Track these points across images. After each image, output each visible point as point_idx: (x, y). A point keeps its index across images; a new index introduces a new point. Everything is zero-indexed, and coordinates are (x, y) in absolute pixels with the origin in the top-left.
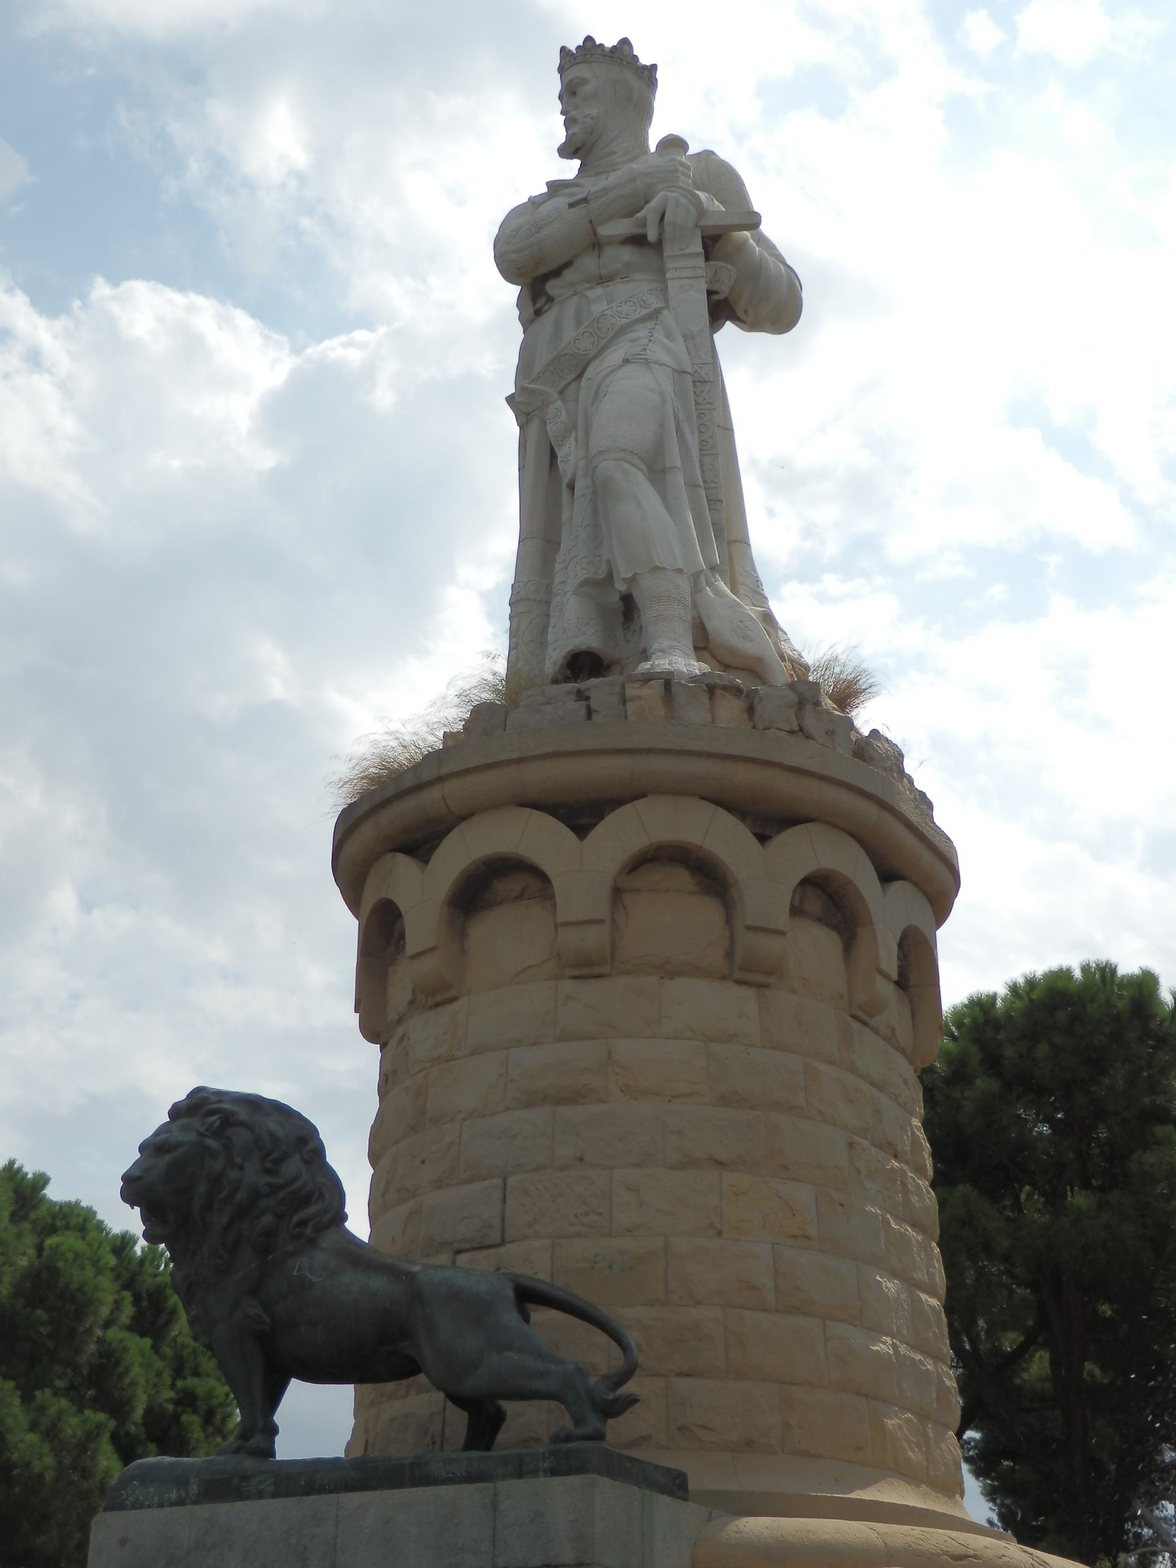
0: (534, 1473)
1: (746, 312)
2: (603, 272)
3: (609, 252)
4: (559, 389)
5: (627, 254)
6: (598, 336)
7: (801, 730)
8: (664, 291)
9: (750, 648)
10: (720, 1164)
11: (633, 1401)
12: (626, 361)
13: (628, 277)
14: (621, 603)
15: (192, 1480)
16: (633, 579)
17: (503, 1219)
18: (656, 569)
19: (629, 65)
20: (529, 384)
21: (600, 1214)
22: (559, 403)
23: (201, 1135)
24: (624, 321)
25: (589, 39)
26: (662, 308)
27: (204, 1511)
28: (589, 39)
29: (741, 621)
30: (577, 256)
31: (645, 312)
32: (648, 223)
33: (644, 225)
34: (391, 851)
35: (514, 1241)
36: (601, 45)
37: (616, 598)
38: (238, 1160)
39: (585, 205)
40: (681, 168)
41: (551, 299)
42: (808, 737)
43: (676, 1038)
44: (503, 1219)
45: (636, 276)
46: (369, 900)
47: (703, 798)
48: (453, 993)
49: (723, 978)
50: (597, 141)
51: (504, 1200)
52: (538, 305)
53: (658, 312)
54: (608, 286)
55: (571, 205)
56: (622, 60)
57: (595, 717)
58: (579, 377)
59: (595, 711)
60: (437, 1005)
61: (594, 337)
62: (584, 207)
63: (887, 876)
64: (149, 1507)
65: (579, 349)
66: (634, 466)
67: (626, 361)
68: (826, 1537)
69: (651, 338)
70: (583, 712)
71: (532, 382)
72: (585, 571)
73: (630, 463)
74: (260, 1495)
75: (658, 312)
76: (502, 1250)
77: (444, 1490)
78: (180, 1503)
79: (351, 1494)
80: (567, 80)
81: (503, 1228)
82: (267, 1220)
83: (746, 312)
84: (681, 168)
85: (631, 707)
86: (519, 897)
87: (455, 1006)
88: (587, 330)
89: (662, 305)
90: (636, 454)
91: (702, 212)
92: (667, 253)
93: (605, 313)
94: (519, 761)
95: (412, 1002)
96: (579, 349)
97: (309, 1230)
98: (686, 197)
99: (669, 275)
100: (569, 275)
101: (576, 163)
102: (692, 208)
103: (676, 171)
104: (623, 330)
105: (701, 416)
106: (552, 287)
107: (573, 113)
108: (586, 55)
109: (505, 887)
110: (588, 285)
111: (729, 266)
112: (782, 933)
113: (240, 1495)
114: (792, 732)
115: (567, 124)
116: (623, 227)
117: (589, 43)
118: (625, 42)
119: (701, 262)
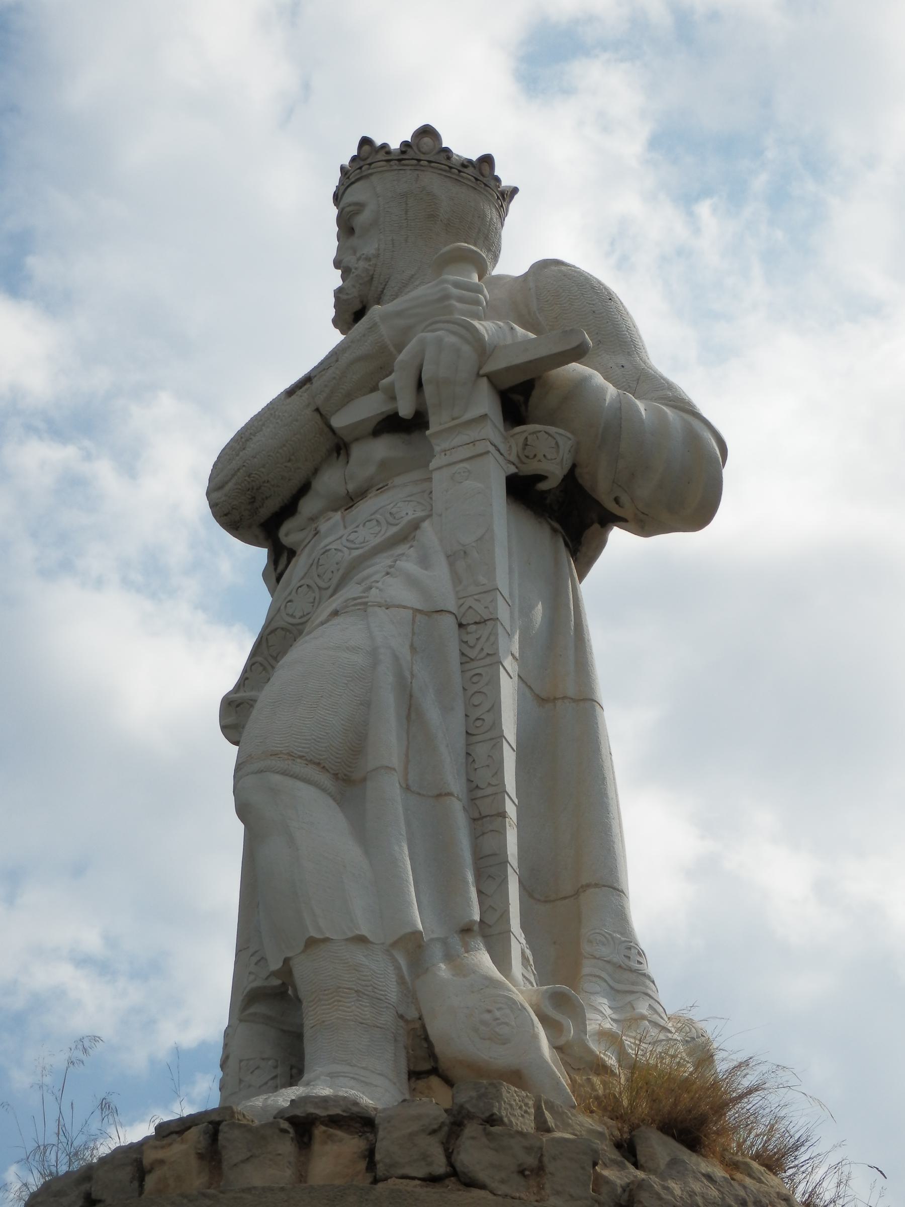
2: (351, 487)
3: (357, 451)
6: (320, 588)
13: (387, 485)
18: (311, 943)
19: (433, 164)
20: (235, 694)
26: (423, 519)
29: (489, 1011)
30: (316, 471)
31: (393, 530)
36: (384, 146)
42: (470, 1183)
45: (398, 480)
50: (382, 292)
53: (415, 526)
56: (419, 160)
61: (314, 592)
62: (307, 390)
65: (292, 616)
66: (296, 777)
69: (390, 570)
72: (252, 977)
73: (284, 773)
75: (415, 526)
83: (617, 500)
85: (150, 1181)
88: (302, 582)
90: (301, 757)
91: (483, 350)
93: (328, 548)
96: (292, 616)
98: (454, 333)
100: (308, 506)
102: (466, 349)
103: (447, 297)
105: (475, 679)
106: (289, 533)
108: (360, 168)
111: (552, 429)
114: (433, 1180)
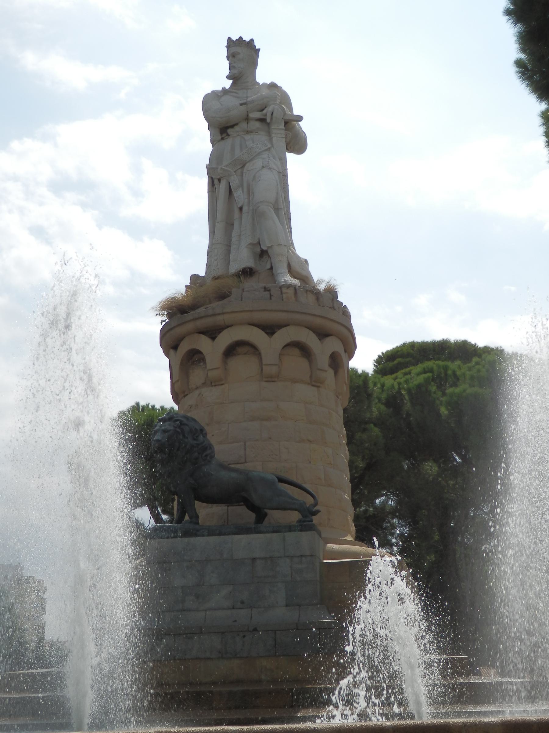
0: (295, 531)
1: (290, 147)
2: (249, 130)
4: (235, 170)
5: (258, 124)
7: (333, 307)
8: (271, 140)
9: (304, 273)
10: (310, 441)
11: (318, 511)
12: (263, 167)
14: (260, 252)
15: (179, 531)
16: (271, 247)
17: (245, 455)
18: (279, 245)
21: (277, 455)
22: (235, 176)
23: (175, 427)
24: (260, 151)
25: (241, 38)
27: (186, 540)
28: (241, 38)
31: (266, 148)
32: (268, 115)
33: (266, 115)
34: (197, 333)
35: (249, 462)
37: (258, 250)
38: (186, 435)
39: (246, 105)
40: (278, 97)
41: (228, 135)
42: (335, 309)
43: (297, 402)
44: (245, 455)
46: (184, 347)
47: (305, 327)
48: (223, 382)
49: (309, 384)
51: (245, 450)
52: (223, 136)
53: (269, 148)
54: (251, 135)
55: (241, 105)
57: (272, 298)
58: (243, 167)
59: (273, 296)
60: (215, 386)
63: (345, 352)
64: (164, 538)
66: (271, 208)
67: (263, 167)
68: (354, 550)
70: (269, 296)
71: (225, 166)
73: (270, 207)
74: (203, 536)
76: (246, 465)
77: (267, 535)
78: (175, 537)
79: (236, 536)
80: (232, 52)
81: (245, 458)
82: (196, 454)
83: (290, 147)
84: (278, 97)
86: (245, 354)
87: (223, 386)
89: (271, 146)
91: (285, 114)
92: (273, 127)
94: (251, 311)
95: (203, 384)
97: (208, 458)
99: (273, 135)
100: (237, 128)
101: (231, 81)
104: (259, 154)
106: (230, 131)
107: (234, 65)
108: (239, 44)
109: (240, 350)
110: (243, 133)
111: (290, 133)
112: (326, 371)
113: (196, 535)
114: (331, 308)
115: (231, 68)
116: (258, 115)
117: (241, 39)
118: (252, 40)
119: (283, 132)
